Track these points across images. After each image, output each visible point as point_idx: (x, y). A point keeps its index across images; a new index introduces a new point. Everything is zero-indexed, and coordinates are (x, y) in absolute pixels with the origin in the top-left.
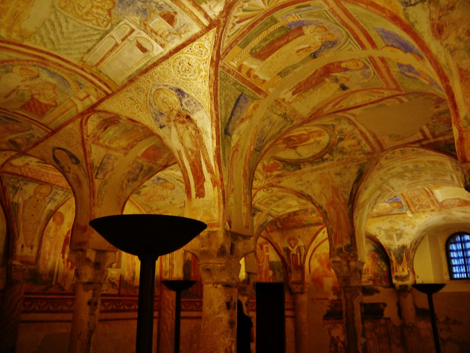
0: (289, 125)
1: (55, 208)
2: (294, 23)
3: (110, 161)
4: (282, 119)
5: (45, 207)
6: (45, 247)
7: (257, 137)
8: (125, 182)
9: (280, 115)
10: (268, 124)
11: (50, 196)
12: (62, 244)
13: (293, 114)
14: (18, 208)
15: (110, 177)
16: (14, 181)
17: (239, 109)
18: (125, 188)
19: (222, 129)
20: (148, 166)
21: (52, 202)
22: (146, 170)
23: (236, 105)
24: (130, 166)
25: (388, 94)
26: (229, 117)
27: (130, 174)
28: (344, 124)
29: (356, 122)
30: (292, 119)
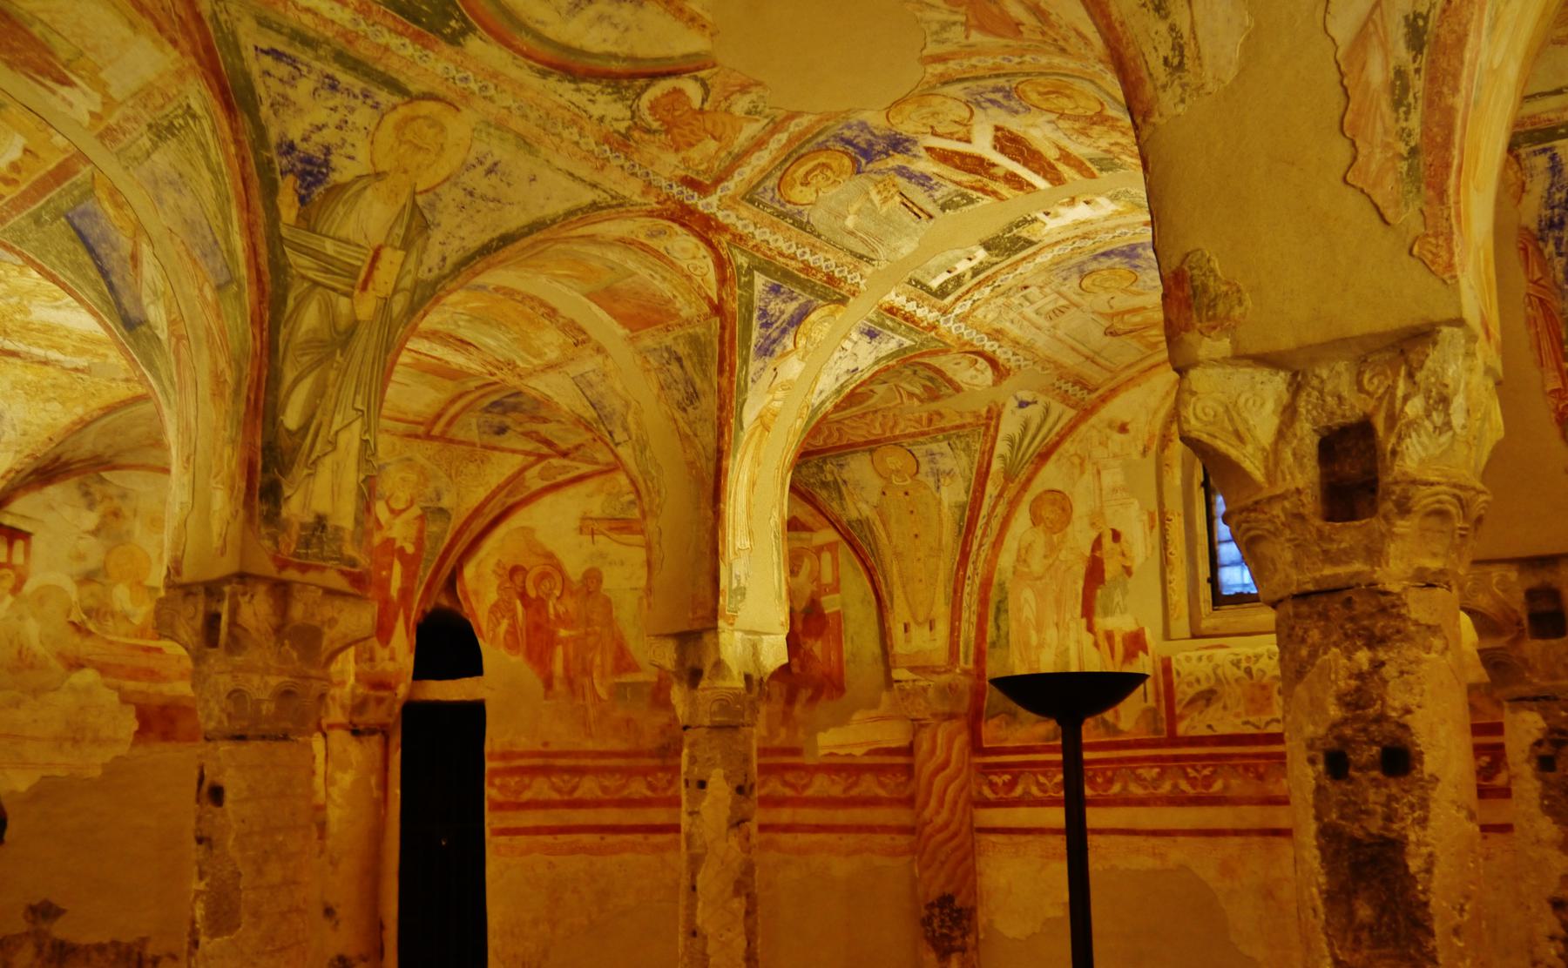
0: (203, 130)
1: (967, 492)
3: (602, 389)
4: (173, 143)
5: (940, 503)
6: (1020, 610)
7: (197, 253)
8: (678, 415)
9: (155, 147)
10: (176, 195)
11: (924, 468)
12: (1081, 583)
13: (159, 101)
14: (872, 532)
15: (639, 424)
16: (811, 471)
17: (104, 245)
18: (691, 434)
19: (117, 328)
20: (681, 341)
21: (945, 481)
22: (689, 355)
23: (91, 250)
24: (649, 370)
26: (106, 289)
27: (669, 388)
30: (180, 112)
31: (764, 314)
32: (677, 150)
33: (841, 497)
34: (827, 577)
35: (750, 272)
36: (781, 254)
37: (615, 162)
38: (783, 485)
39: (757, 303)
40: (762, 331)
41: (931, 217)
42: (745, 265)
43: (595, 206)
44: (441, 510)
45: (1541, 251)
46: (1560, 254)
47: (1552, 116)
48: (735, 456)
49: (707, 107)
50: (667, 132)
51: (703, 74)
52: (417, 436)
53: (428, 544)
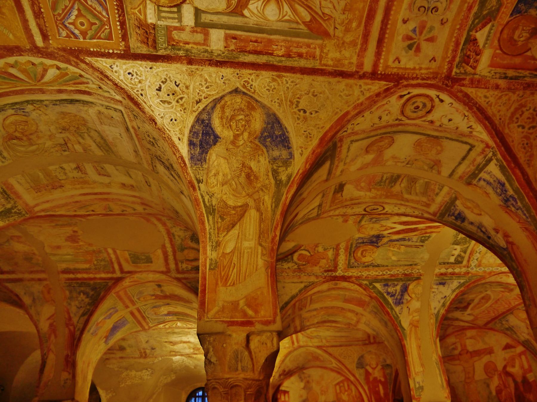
2: (170, 316)
14: (532, 344)
25: (126, 282)
28: (179, 236)
29: (166, 236)
31: (388, 293)
32: (316, 266)
33: (516, 333)
34: (526, 366)
35: (371, 284)
36: (378, 276)
37: (302, 275)
38: (435, 343)
39: (382, 291)
40: (392, 298)
41: (422, 246)
43: (306, 287)
44: (388, 365)
45: (511, 211)
46: (517, 209)
47: (469, 170)
48: (406, 340)
49: (312, 254)
50: (309, 263)
51: (302, 248)
52: (367, 344)
53: (388, 377)
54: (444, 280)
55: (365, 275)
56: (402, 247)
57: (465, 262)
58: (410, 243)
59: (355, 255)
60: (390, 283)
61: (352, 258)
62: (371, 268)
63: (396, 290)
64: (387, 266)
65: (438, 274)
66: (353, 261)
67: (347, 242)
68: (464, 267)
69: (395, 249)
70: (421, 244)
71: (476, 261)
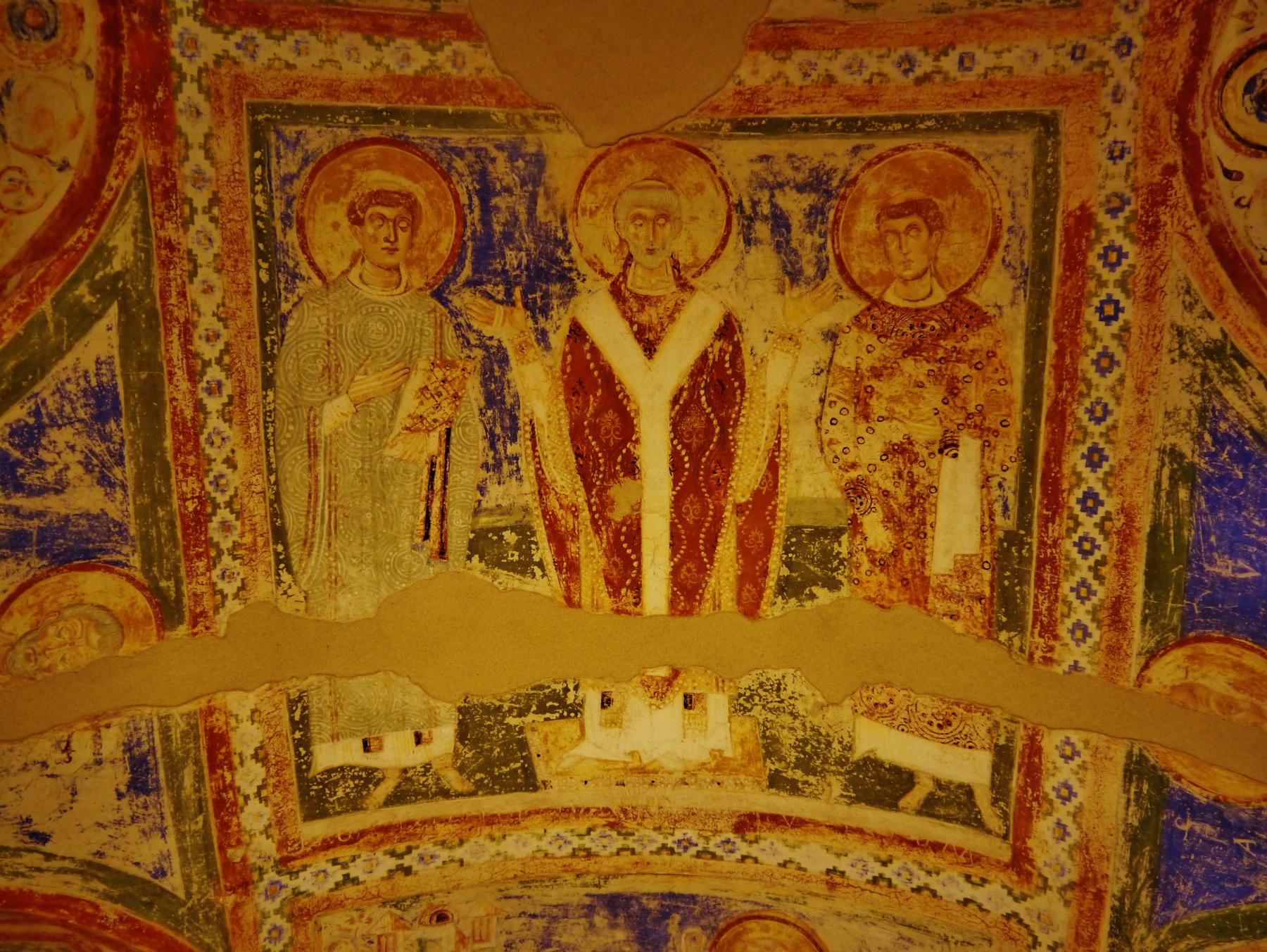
35: (109, 289)
39: (45, 388)
41: (442, 553)
42: (117, 265)
54: (174, 771)
55: (188, 240)
56: (433, 443)
57: (319, 829)
58: (465, 475)
59: (370, 152)
60: (122, 429)
61: (345, 135)
62: (256, 272)
63: (60, 487)
64: (268, 383)
65: (218, 720)
66: (318, 139)
67: (490, 89)
68: (282, 845)
69: (409, 404)
70: (458, 543)
71: (337, 874)
